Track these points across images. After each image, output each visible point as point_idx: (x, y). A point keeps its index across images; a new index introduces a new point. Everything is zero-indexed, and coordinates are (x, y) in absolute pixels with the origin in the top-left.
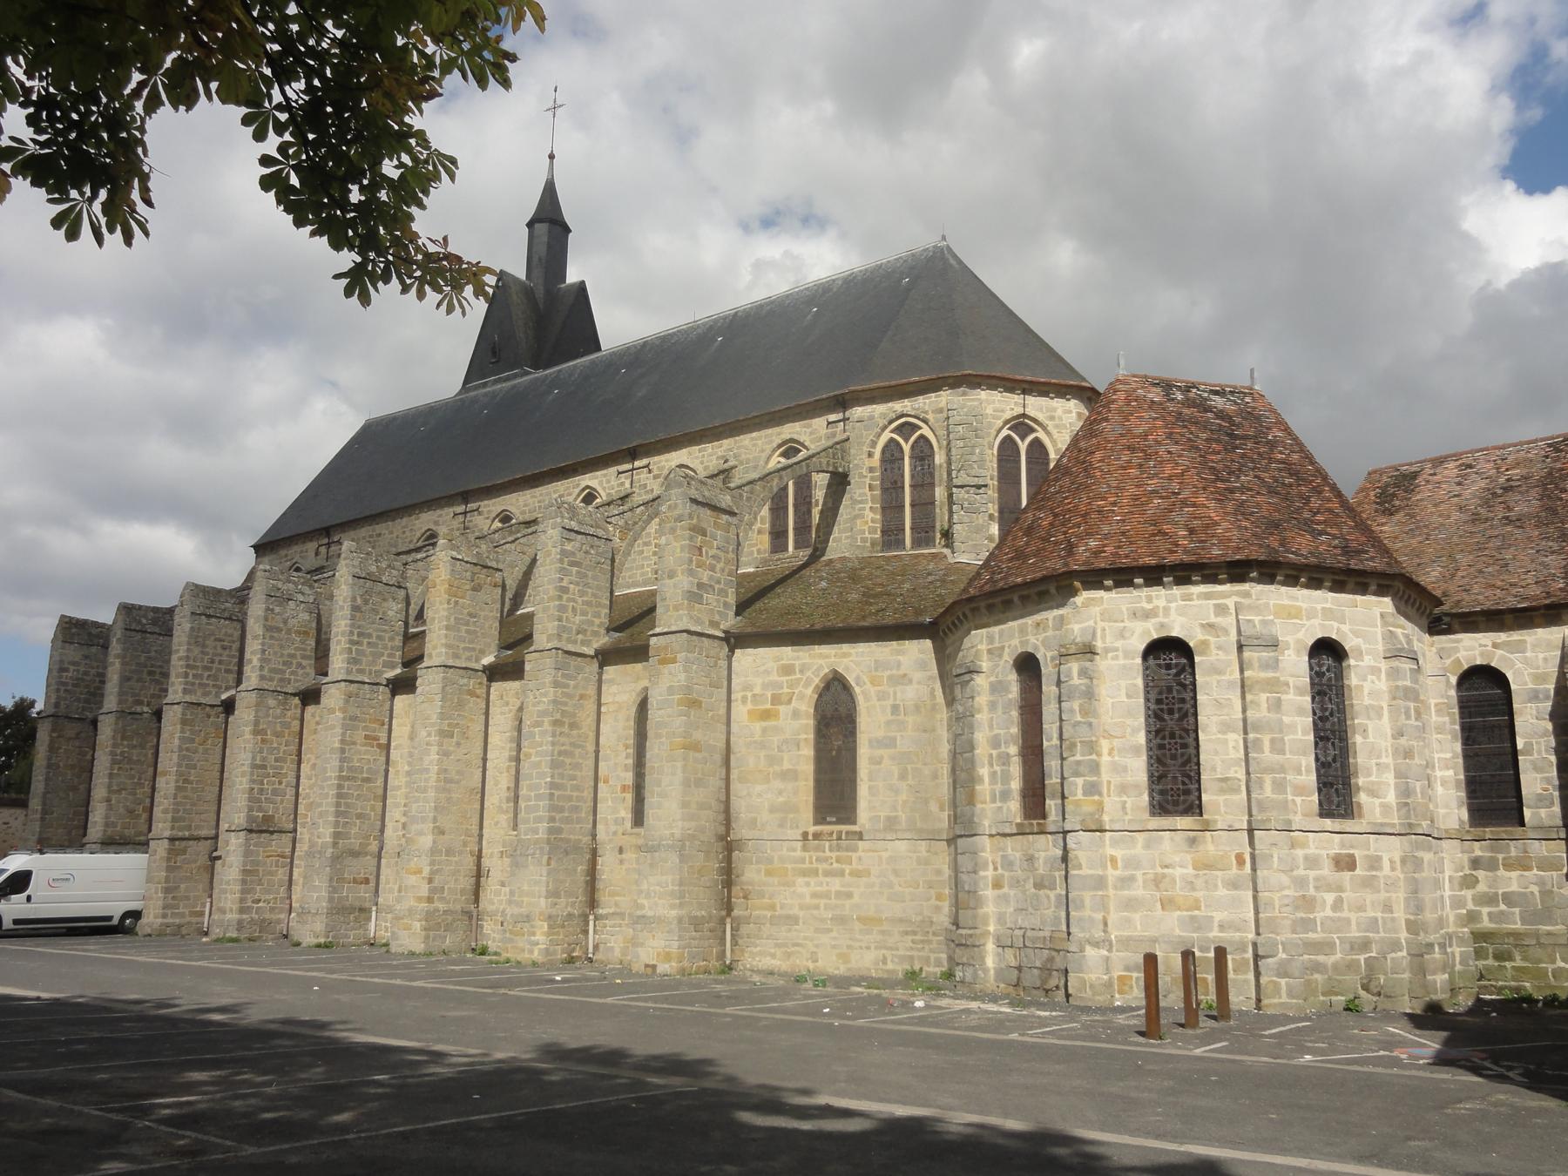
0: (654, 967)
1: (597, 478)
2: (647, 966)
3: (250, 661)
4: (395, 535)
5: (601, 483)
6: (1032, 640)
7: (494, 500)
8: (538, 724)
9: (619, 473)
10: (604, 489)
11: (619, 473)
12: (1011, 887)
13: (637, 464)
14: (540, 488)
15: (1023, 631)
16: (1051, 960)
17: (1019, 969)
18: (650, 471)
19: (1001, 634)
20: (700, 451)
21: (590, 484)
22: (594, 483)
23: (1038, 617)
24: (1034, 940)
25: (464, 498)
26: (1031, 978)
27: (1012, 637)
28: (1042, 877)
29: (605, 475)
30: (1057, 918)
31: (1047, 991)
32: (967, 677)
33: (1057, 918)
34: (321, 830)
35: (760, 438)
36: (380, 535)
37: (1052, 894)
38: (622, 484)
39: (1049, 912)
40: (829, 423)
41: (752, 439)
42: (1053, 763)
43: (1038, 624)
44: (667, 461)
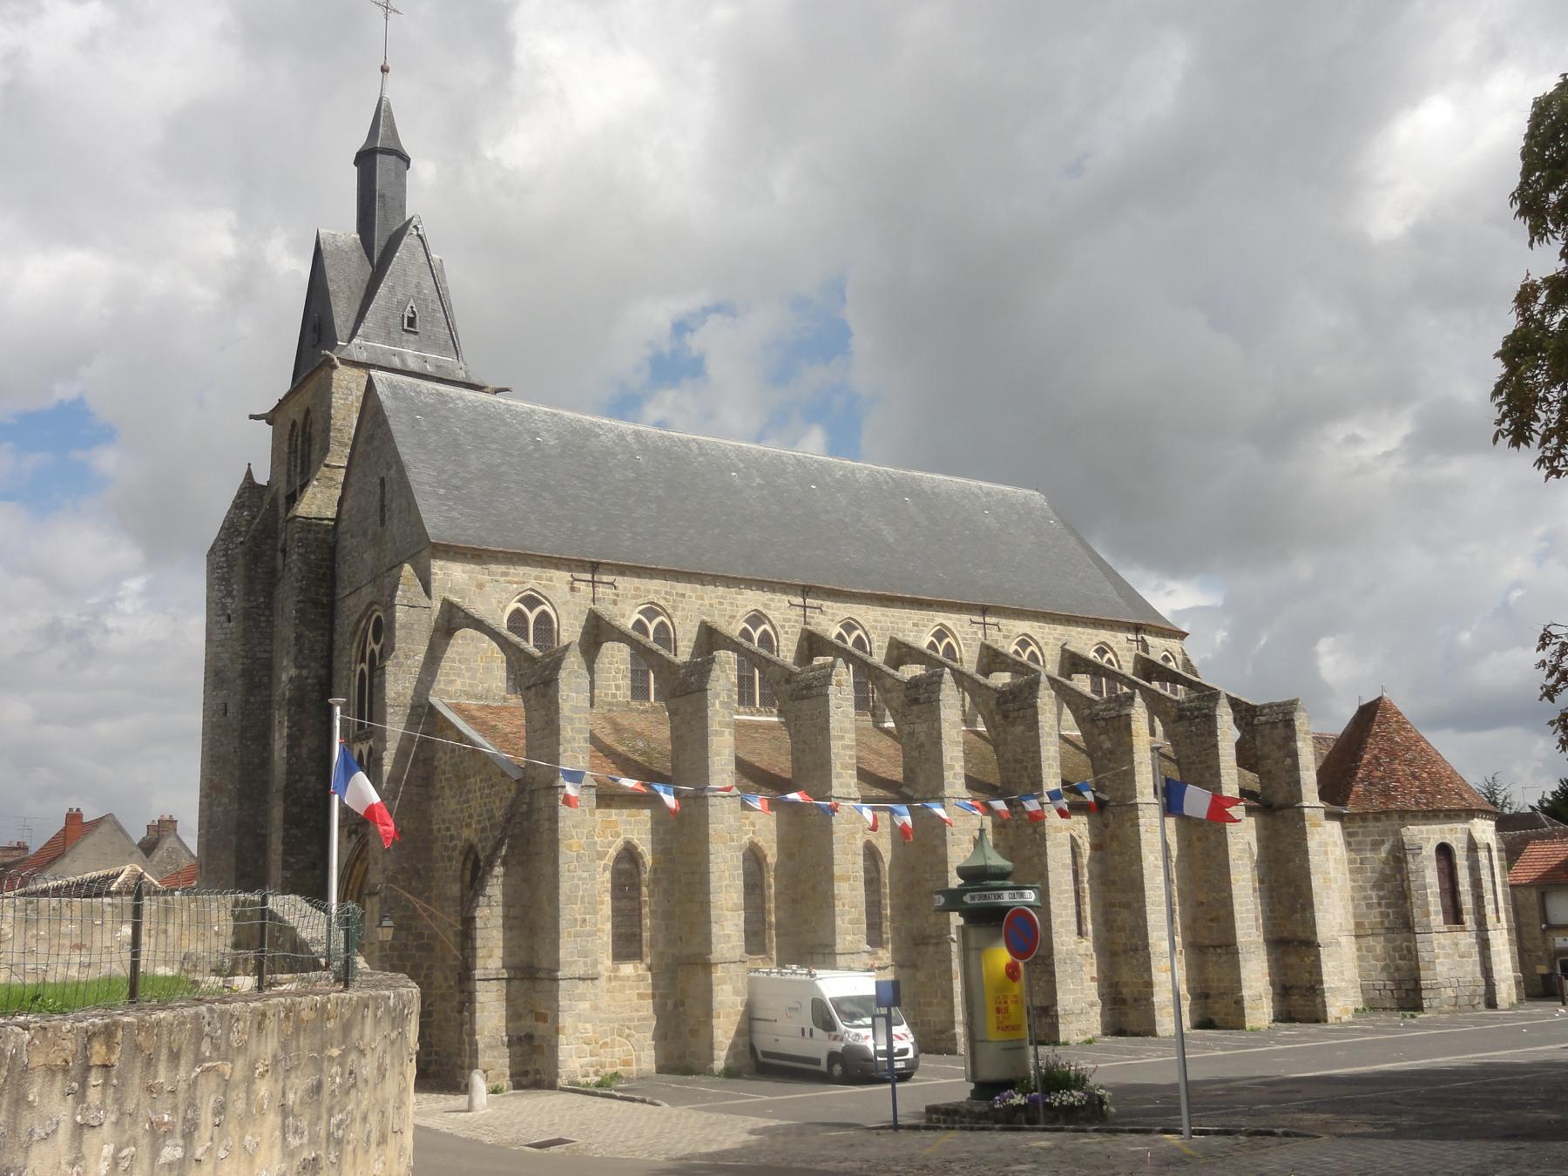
0: (1340, 1018)
1: (950, 619)
2: (1336, 1018)
3: (952, 767)
4: (707, 602)
5: (955, 624)
6: (1448, 837)
7: (839, 605)
8: (1240, 858)
9: (973, 622)
10: (959, 631)
11: (973, 622)
12: (1445, 957)
13: (988, 620)
14: (892, 610)
15: (1442, 831)
16: (1475, 991)
17: (1456, 997)
18: (999, 630)
19: (1428, 831)
20: (1040, 627)
21: (944, 622)
22: (949, 624)
23: (1451, 826)
24: (1464, 983)
25: (803, 591)
26: (1463, 1000)
27: (1434, 833)
28: (1464, 952)
29: (959, 620)
30: (1474, 972)
31: (1473, 1006)
32: (1418, 851)
33: (1474, 972)
34: (1064, 938)
35: (1083, 633)
36: (683, 595)
37: (1470, 960)
38: (975, 633)
39: (1469, 969)
40: (1128, 640)
41: (1079, 633)
42: (1466, 898)
43: (1451, 830)
44: (1014, 626)
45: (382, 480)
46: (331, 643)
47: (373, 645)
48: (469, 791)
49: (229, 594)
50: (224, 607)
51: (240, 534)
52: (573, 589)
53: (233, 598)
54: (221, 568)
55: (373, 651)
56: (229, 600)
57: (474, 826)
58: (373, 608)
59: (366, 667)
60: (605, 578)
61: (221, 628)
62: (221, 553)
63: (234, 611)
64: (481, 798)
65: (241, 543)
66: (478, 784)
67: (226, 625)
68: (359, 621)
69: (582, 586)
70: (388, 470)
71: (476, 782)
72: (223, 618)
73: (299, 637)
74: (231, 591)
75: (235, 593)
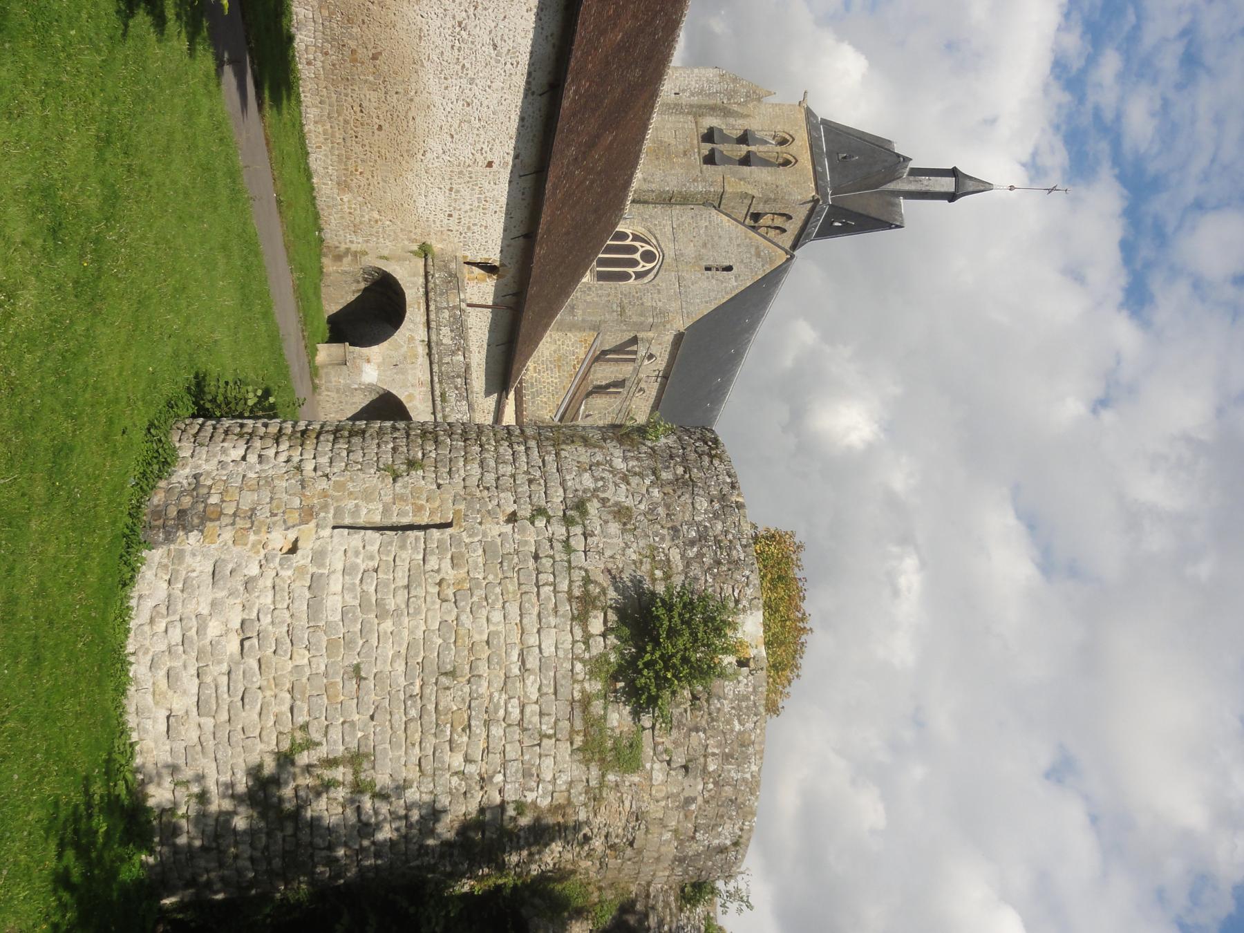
45: (729, 269)
46: (646, 202)
47: (641, 250)
48: (552, 370)
49: (692, 94)
50: (684, 91)
51: (729, 99)
52: (654, 371)
53: (689, 97)
54: (709, 89)
55: (634, 250)
56: (688, 94)
57: (535, 375)
58: (661, 254)
59: (628, 242)
60: (659, 380)
61: (671, 89)
62: (718, 89)
63: (680, 97)
64: (548, 383)
65: (723, 103)
66: (555, 381)
67: (673, 92)
68: (656, 238)
69: (657, 373)
70: (736, 277)
71: (556, 378)
72: (677, 91)
73: (653, 191)
74: (693, 96)
75: (692, 98)
